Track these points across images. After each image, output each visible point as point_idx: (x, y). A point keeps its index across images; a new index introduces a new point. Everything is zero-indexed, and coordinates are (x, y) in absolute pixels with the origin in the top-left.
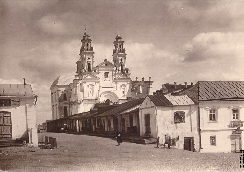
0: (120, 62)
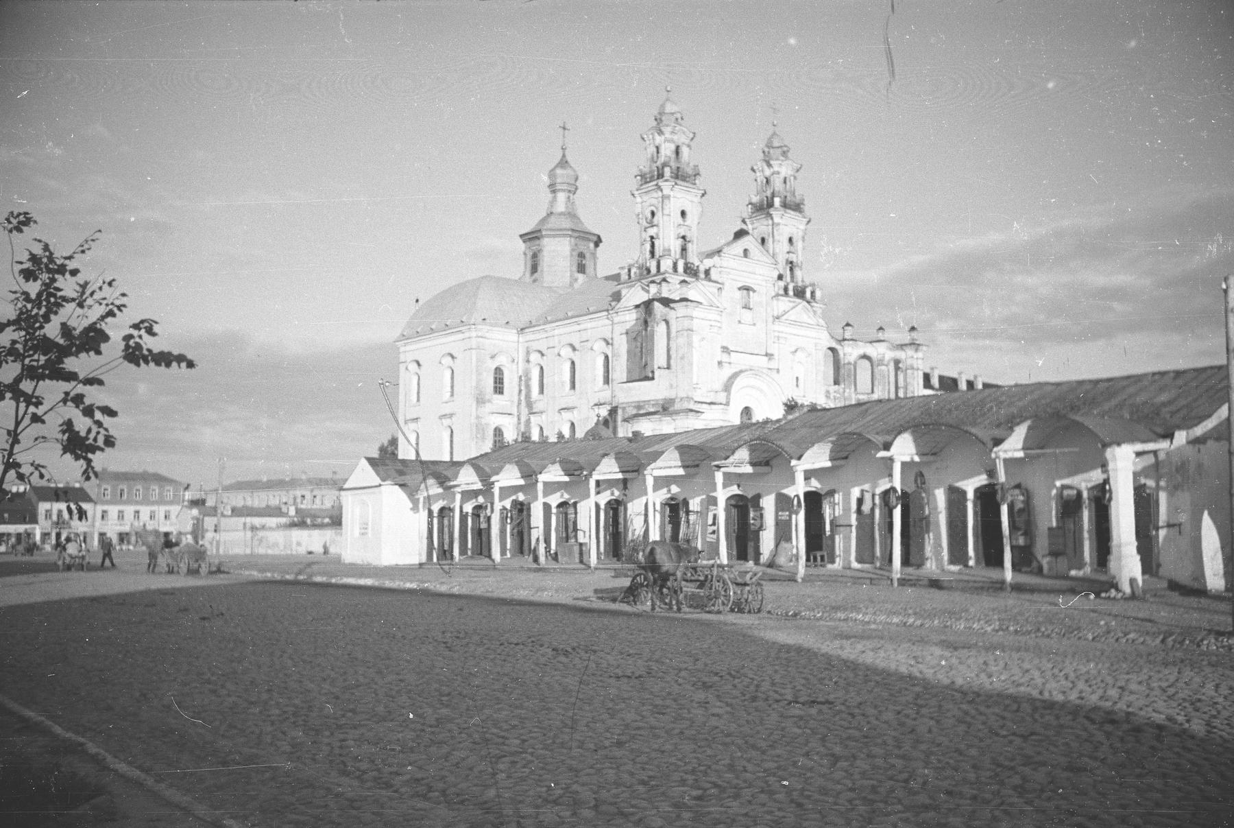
0: (786, 246)
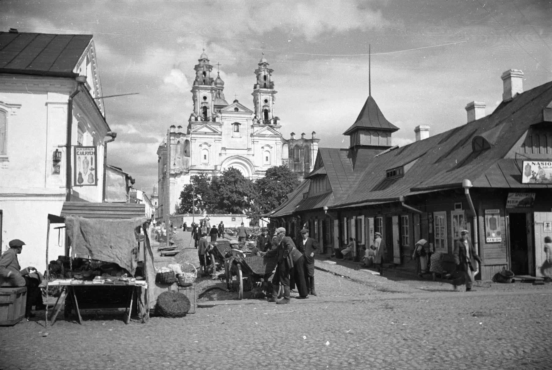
0: (263, 104)
